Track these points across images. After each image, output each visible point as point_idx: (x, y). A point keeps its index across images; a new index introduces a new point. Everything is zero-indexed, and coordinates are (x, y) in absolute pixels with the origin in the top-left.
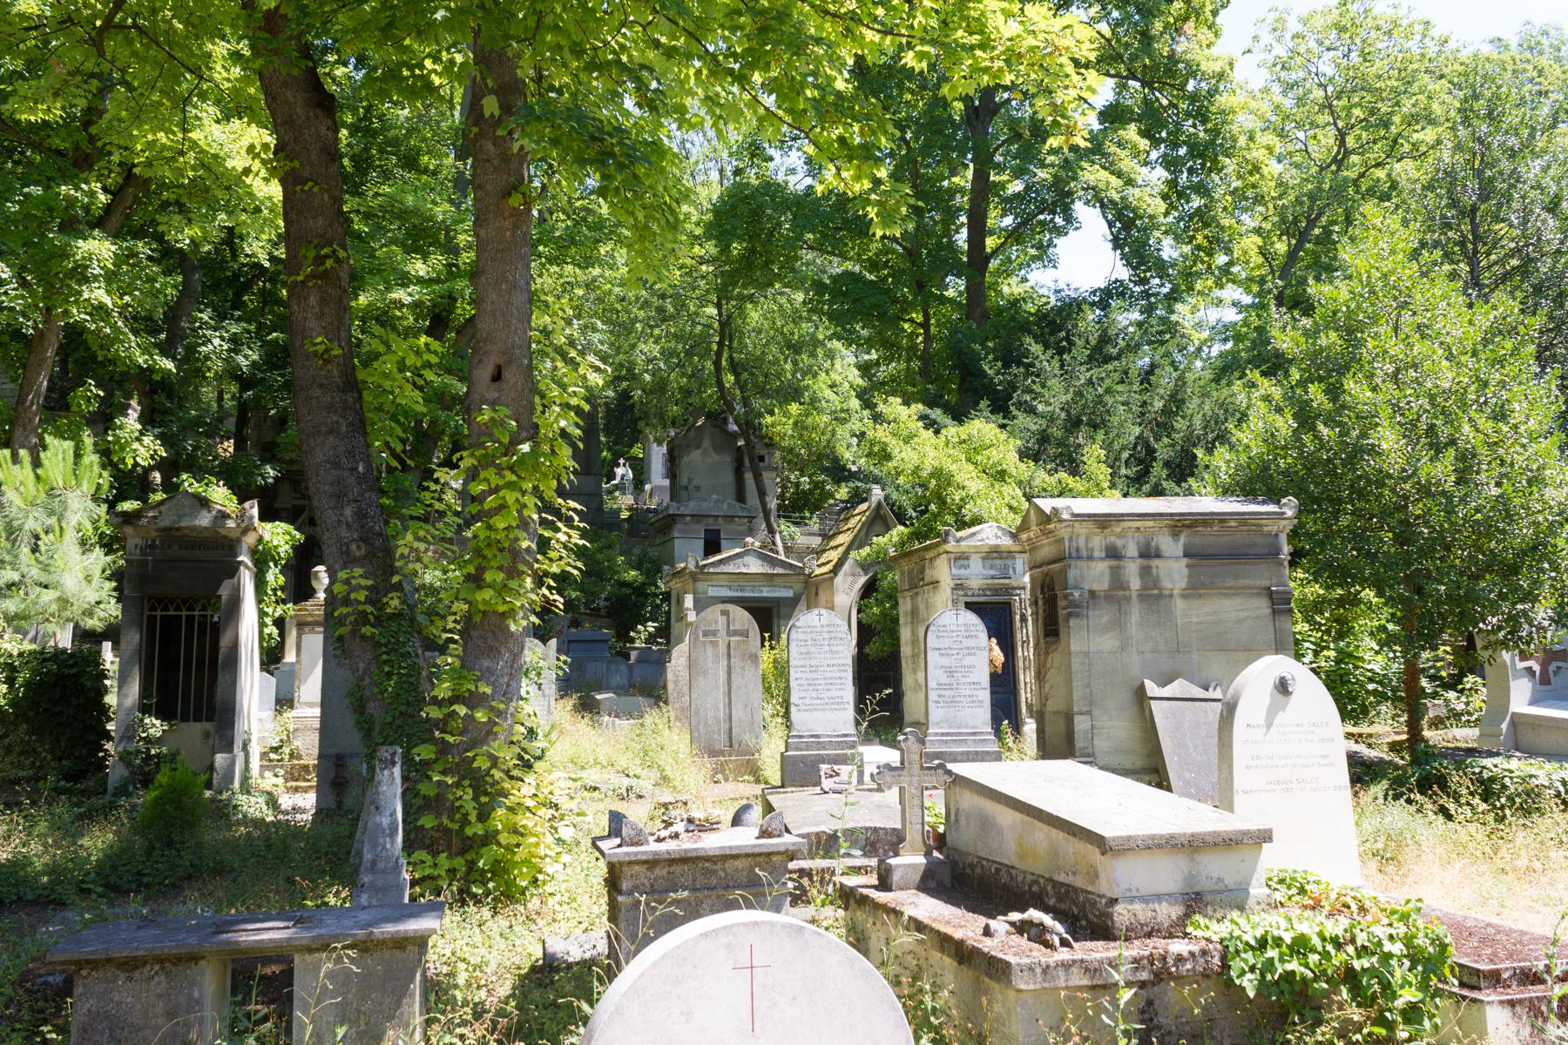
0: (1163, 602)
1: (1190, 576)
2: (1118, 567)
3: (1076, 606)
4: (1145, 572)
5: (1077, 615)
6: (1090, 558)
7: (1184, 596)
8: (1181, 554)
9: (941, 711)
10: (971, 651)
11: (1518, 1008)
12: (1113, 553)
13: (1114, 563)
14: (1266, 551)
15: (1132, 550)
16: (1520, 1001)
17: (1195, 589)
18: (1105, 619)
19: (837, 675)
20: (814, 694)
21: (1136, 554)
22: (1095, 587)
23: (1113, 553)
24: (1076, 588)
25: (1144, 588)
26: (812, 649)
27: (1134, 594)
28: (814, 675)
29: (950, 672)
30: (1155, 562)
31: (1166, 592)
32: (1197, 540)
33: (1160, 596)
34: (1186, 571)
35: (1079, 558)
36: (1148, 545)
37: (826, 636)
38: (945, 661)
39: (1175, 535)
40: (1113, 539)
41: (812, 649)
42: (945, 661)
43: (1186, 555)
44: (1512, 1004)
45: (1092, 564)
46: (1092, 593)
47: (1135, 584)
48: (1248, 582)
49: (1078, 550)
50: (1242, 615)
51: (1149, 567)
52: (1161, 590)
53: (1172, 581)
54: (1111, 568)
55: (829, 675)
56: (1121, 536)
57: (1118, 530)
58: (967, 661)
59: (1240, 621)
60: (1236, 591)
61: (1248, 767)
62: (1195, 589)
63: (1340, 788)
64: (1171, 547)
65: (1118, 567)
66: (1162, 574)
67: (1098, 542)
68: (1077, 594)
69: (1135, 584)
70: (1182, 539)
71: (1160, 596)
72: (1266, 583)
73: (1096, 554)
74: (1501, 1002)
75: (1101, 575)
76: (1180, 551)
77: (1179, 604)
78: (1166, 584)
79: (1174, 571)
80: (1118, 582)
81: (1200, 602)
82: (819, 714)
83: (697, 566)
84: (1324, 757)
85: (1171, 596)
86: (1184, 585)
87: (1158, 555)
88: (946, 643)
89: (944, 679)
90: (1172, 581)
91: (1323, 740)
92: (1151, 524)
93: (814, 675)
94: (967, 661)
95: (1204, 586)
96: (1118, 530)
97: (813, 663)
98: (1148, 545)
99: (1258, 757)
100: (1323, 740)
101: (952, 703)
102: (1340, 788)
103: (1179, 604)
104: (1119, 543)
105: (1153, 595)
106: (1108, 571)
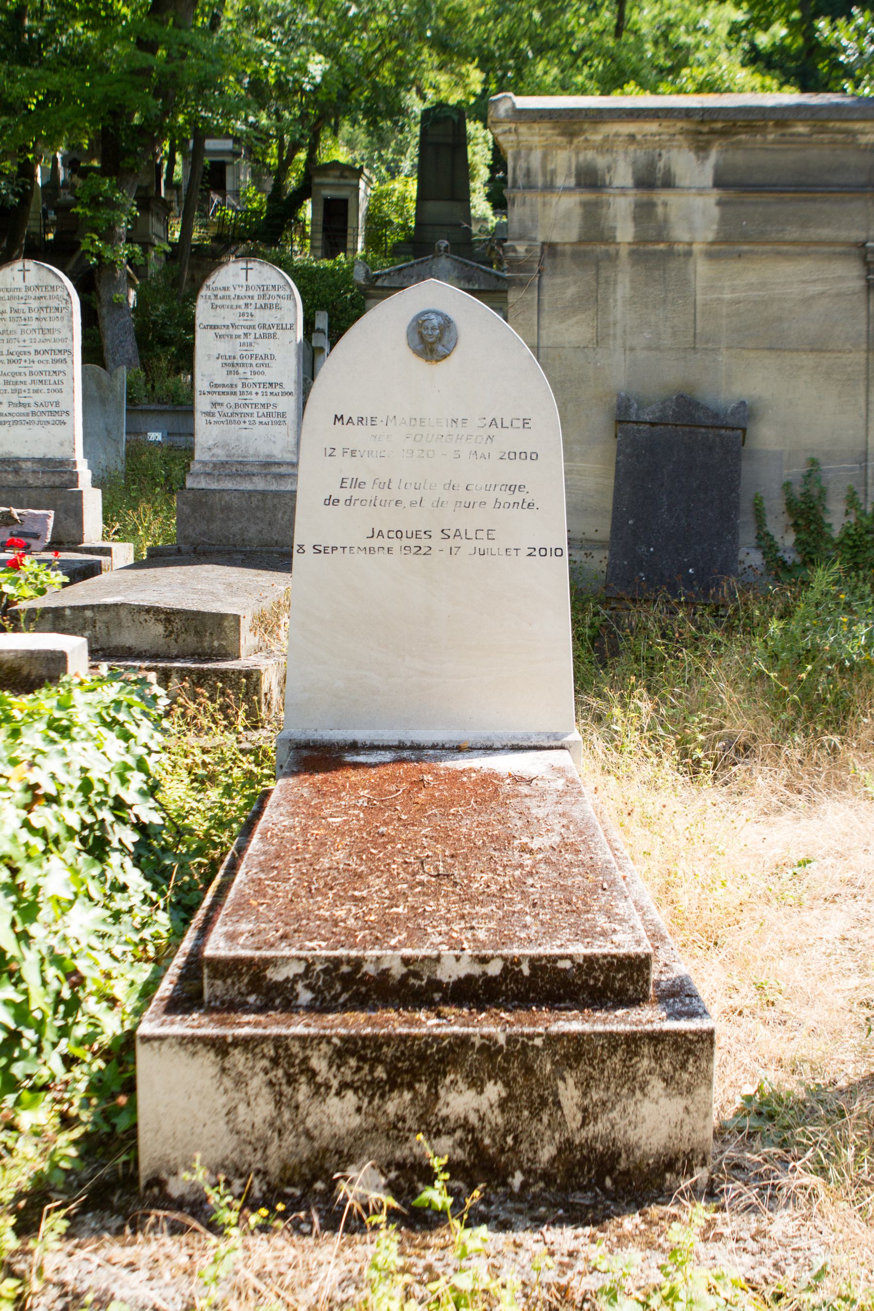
0: (673, 264)
1: (723, 220)
2: (597, 204)
3: (521, 269)
4: (644, 212)
5: (522, 284)
6: (549, 187)
7: (710, 255)
8: (710, 182)
9: (216, 430)
10: (268, 332)
11: (238, 1057)
12: (590, 180)
13: (590, 196)
14: (862, 179)
15: (623, 175)
16: (247, 1044)
17: (730, 244)
18: (571, 291)
19: (50, 367)
20: (15, 398)
21: (629, 182)
22: (556, 237)
23: (590, 180)
24: (521, 238)
25: (640, 240)
26: (12, 326)
27: (624, 251)
28: (15, 368)
29: (231, 365)
30: (661, 196)
31: (680, 248)
32: (739, 158)
33: (670, 254)
34: (716, 212)
35: (530, 187)
36: (651, 166)
37: (34, 304)
38: (224, 347)
39: (701, 149)
40: (590, 154)
41: (12, 326)
42: (224, 347)
43: (719, 183)
44: (220, 1047)
45: (553, 199)
46: (550, 249)
47: (625, 232)
48: (826, 233)
49: (528, 173)
50: (813, 289)
51: (651, 205)
52: (671, 243)
53: (691, 229)
54: (584, 204)
55: (37, 367)
56: (606, 147)
57: (597, 138)
58: (262, 347)
59: (807, 301)
60: (805, 249)
61: (331, 501)
62: (730, 244)
63: (543, 552)
64: (693, 169)
65: (597, 204)
66: (674, 214)
67: (564, 161)
68: (521, 249)
69: (625, 232)
70: (713, 156)
71: (670, 254)
72: (858, 235)
73: (560, 182)
74: (185, 1041)
75: (567, 215)
76: (707, 176)
77: (702, 269)
78: (680, 233)
79: (694, 210)
80: (595, 230)
81: (739, 265)
82: (21, 430)
83: (367, 277)
84: (512, 489)
85: (689, 254)
86: (711, 236)
87: (668, 183)
88: (227, 317)
89: (221, 377)
90: (691, 229)
91: (513, 456)
92: (652, 127)
93: (15, 368)
94: (262, 347)
95: (746, 238)
96: (597, 138)
97: (15, 347)
98: (651, 166)
99: (357, 484)
100: (513, 456)
101: (233, 417)
102: (543, 552)
103: (702, 269)
104: (601, 162)
105: (656, 251)
106: (578, 211)
